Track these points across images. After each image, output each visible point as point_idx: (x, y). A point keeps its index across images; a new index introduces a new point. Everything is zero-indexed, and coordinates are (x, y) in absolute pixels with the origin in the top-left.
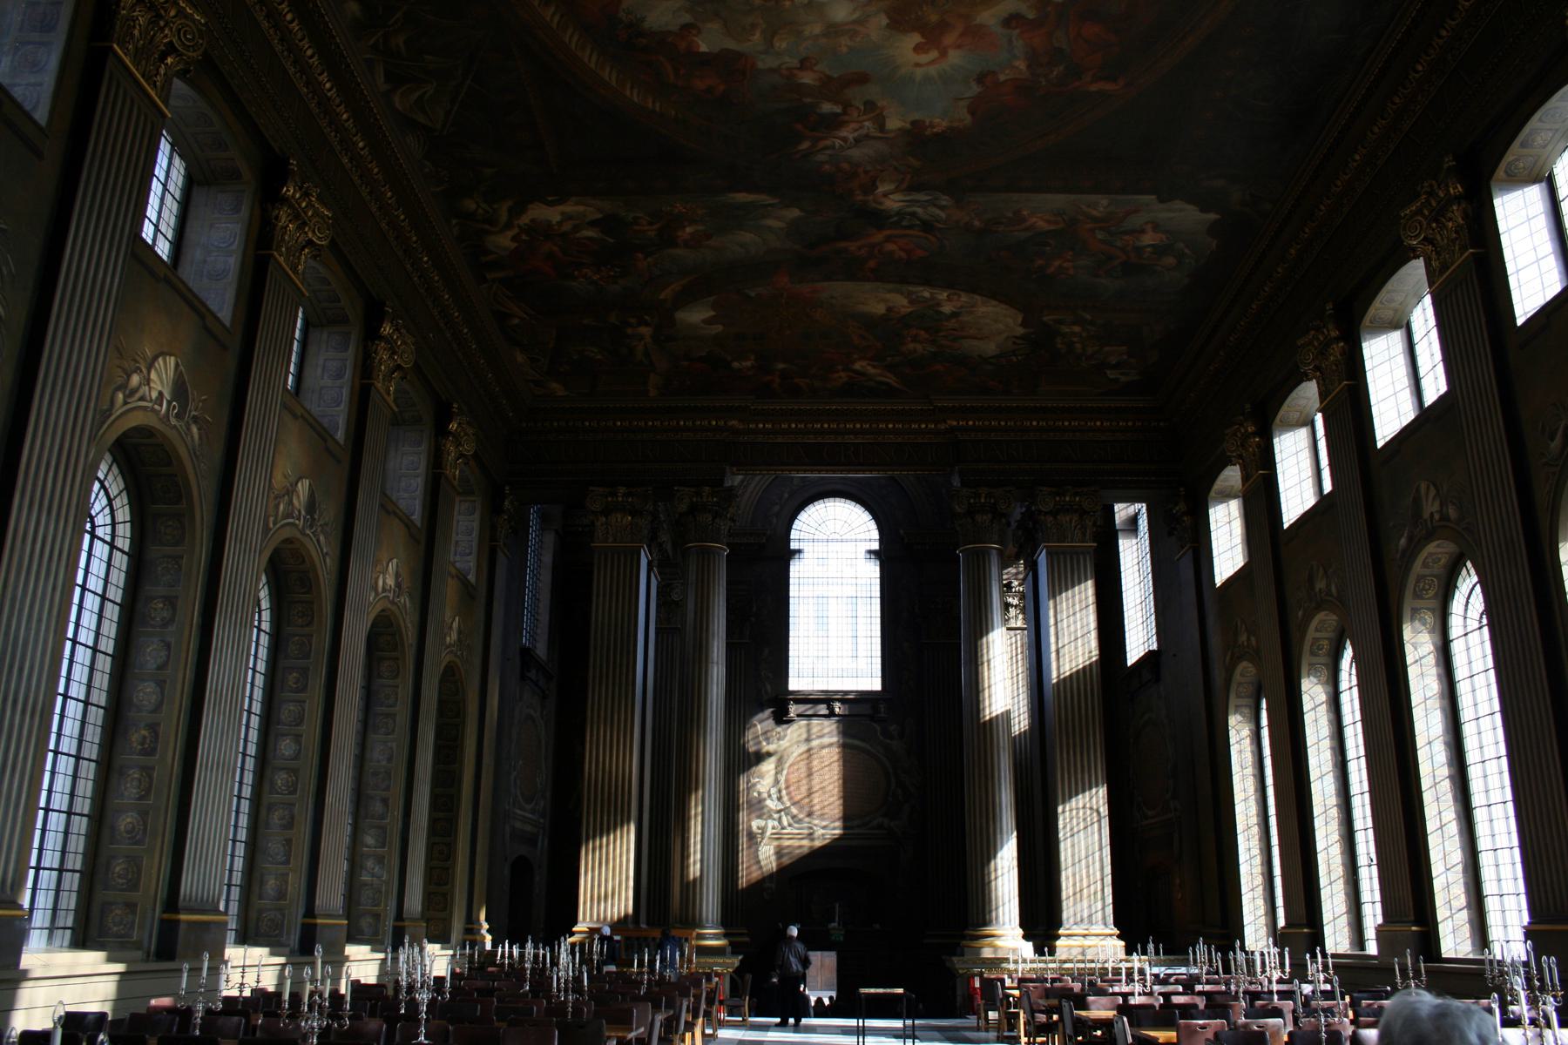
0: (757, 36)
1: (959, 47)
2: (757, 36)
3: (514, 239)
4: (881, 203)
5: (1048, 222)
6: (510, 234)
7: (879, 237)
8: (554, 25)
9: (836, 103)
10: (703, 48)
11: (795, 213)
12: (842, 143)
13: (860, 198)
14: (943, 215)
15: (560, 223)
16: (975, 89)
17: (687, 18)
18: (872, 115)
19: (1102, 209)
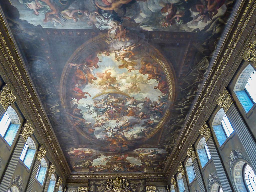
0: (138, 77)
1: (103, 74)
2: (138, 77)
3: (216, 12)
4: (114, 24)
5: (67, 16)
6: (216, 16)
7: (114, 6)
8: (171, 81)
9: (125, 61)
10: (148, 75)
11: (137, 20)
12: (124, 49)
13: (120, 27)
14: (97, 19)
15: (200, 21)
16: (98, 64)
17: (149, 81)
18: (118, 58)
19: (55, 22)
